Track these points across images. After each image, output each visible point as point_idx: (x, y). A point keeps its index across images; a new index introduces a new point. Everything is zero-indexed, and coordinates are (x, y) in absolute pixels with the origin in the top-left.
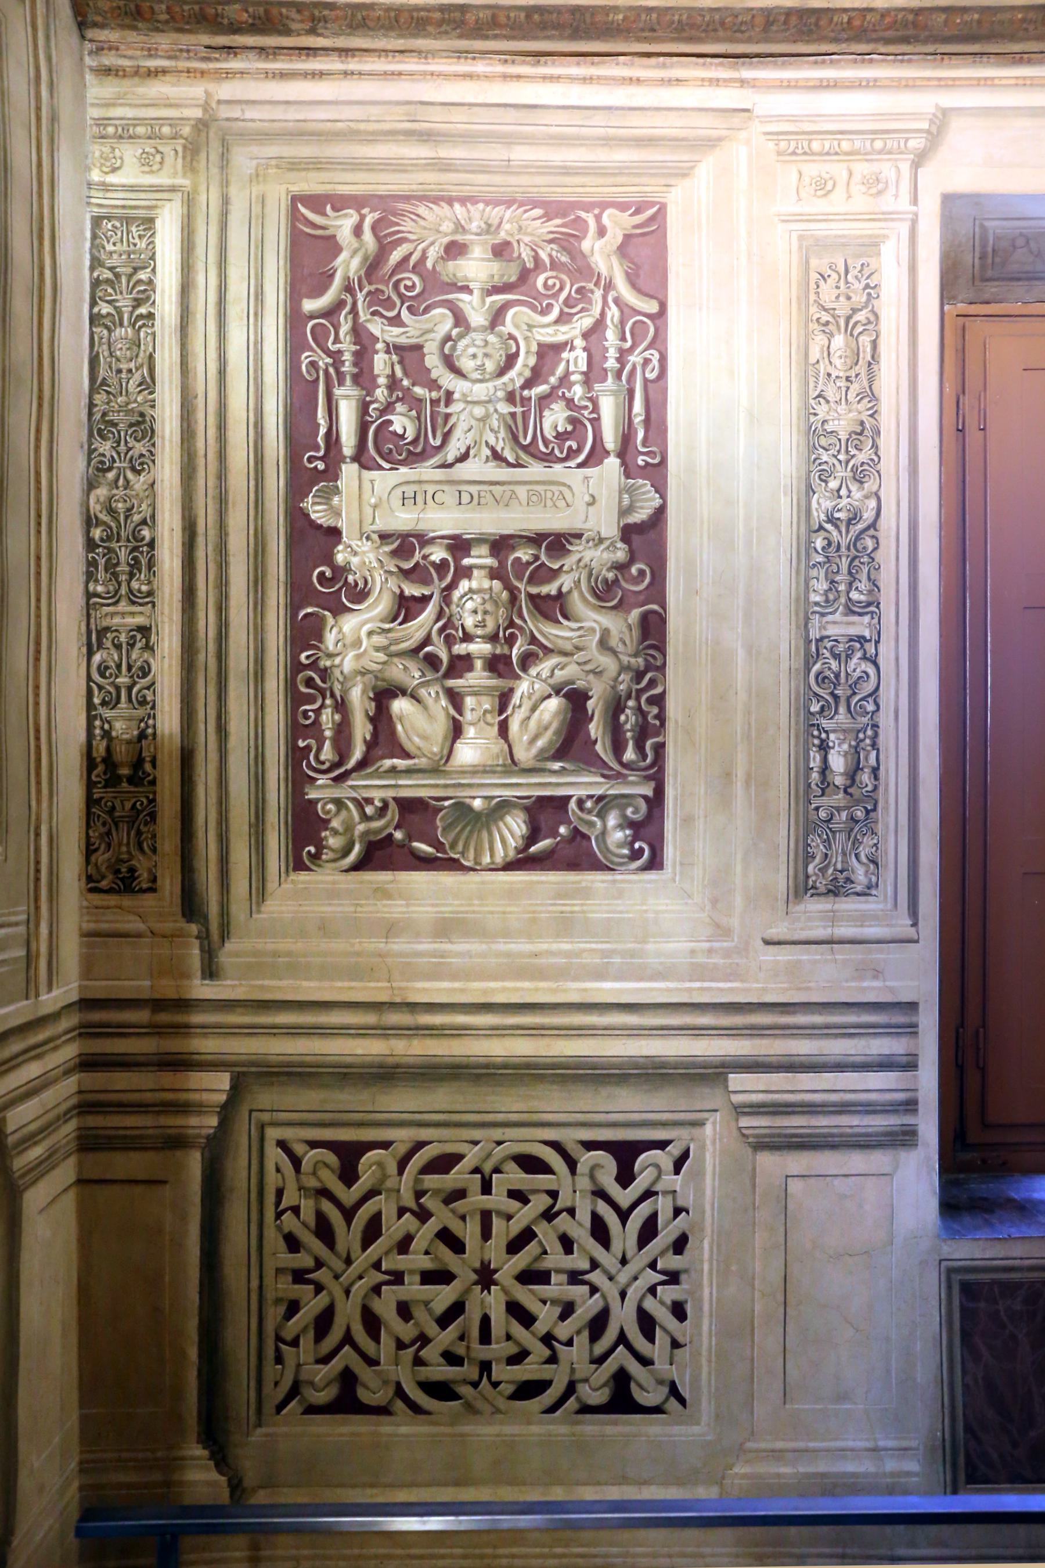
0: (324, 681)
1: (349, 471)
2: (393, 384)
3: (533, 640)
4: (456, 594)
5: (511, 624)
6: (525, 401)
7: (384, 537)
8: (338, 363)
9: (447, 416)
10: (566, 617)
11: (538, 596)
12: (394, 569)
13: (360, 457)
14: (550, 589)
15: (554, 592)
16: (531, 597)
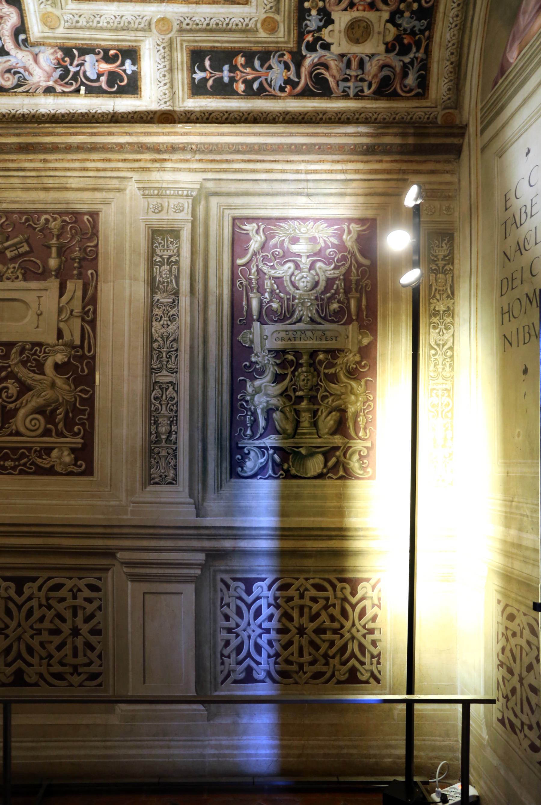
0: (247, 405)
1: (256, 325)
2: (272, 292)
3: (326, 391)
4: (296, 373)
5: (318, 384)
6: (323, 299)
7: (270, 351)
8: (250, 283)
9: (293, 305)
10: (338, 382)
11: (328, 373)
12: (273, 363)
13: (260, 319)
14: (332, 371)
15: (333, 372)
16: (324, 373)
